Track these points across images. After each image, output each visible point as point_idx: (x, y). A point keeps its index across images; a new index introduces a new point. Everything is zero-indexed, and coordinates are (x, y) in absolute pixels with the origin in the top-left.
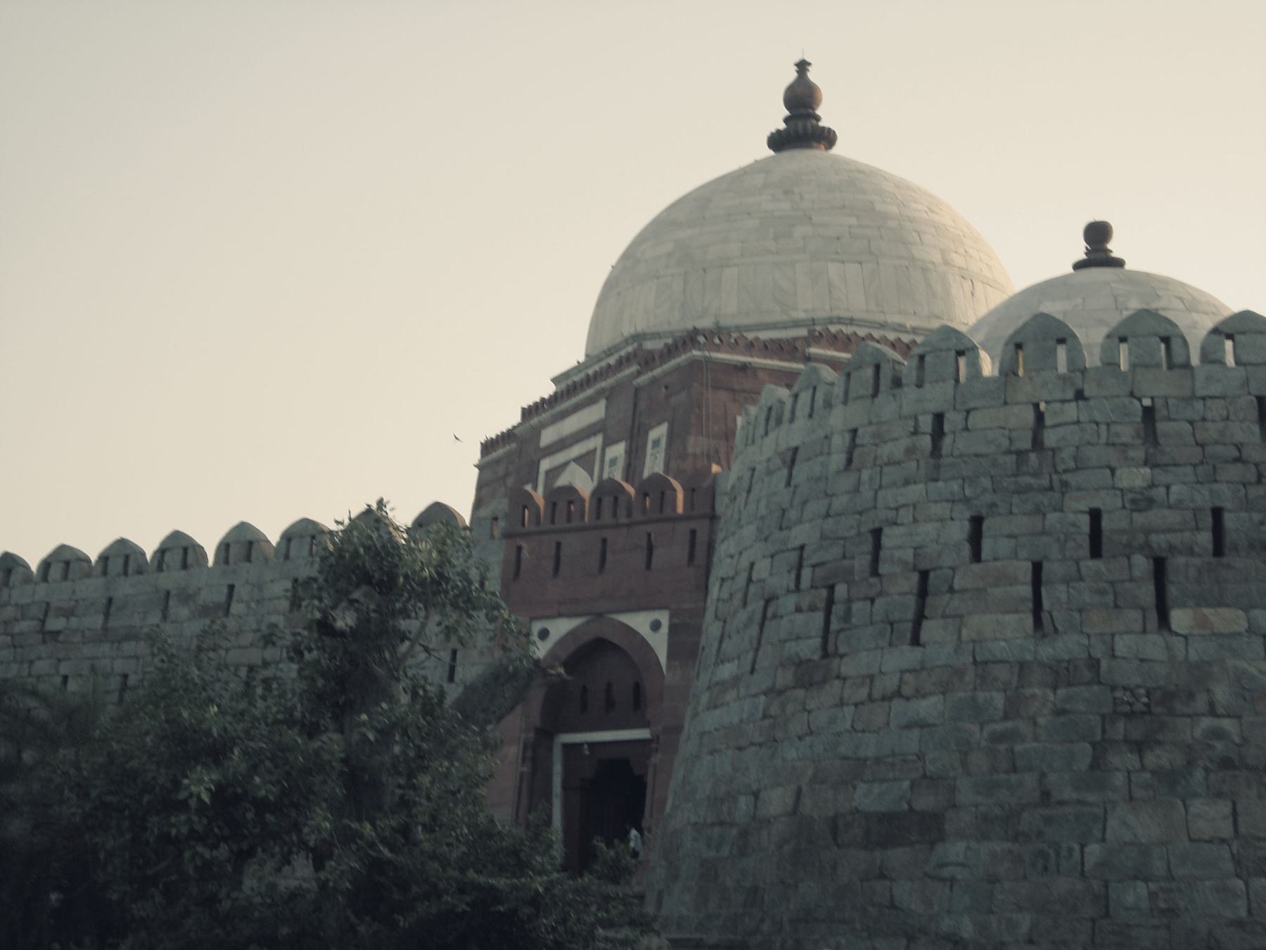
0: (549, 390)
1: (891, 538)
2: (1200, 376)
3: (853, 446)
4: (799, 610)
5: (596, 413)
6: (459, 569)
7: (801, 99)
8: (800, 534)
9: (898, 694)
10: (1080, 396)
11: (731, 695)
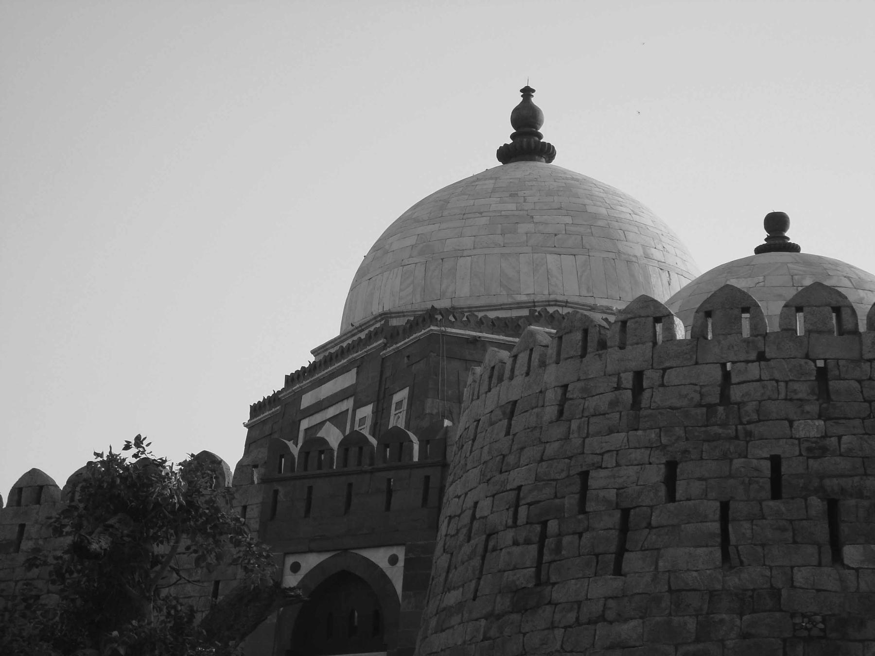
0: (307, 359)
1: (597, 480)
2: (867, 341)
4: (516, 543)
5: (348, 380)
6: (208, 498)
7: (526, 118)
8: (517, 477)
9: (602, 618)
10: (762, 357)
11: (455, 620)
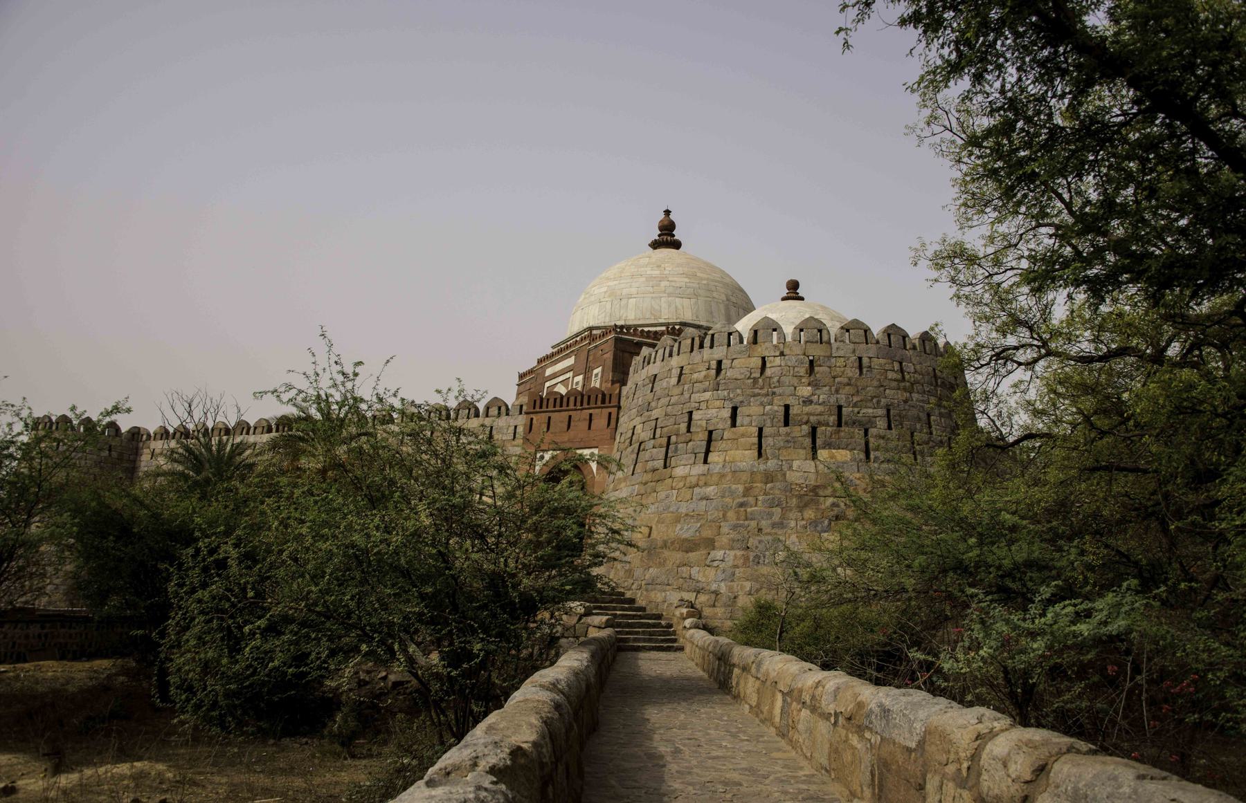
0: (549, 351)
1: (696, 416)
2: (835, 345)
3: (681, 374)
5: (570, 361)
7: (667, 228)
8: (655, 413)
9: (697, 485)
10: (782, 354)
11: (623, 485)
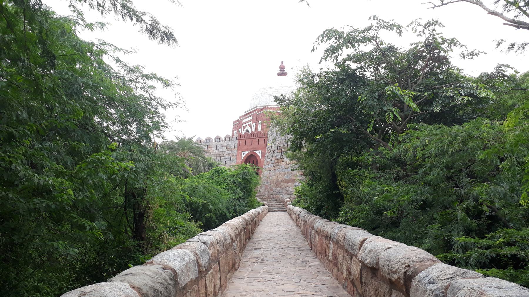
0: (244, 114)
5: (251, 118)
8: (277, 142)
